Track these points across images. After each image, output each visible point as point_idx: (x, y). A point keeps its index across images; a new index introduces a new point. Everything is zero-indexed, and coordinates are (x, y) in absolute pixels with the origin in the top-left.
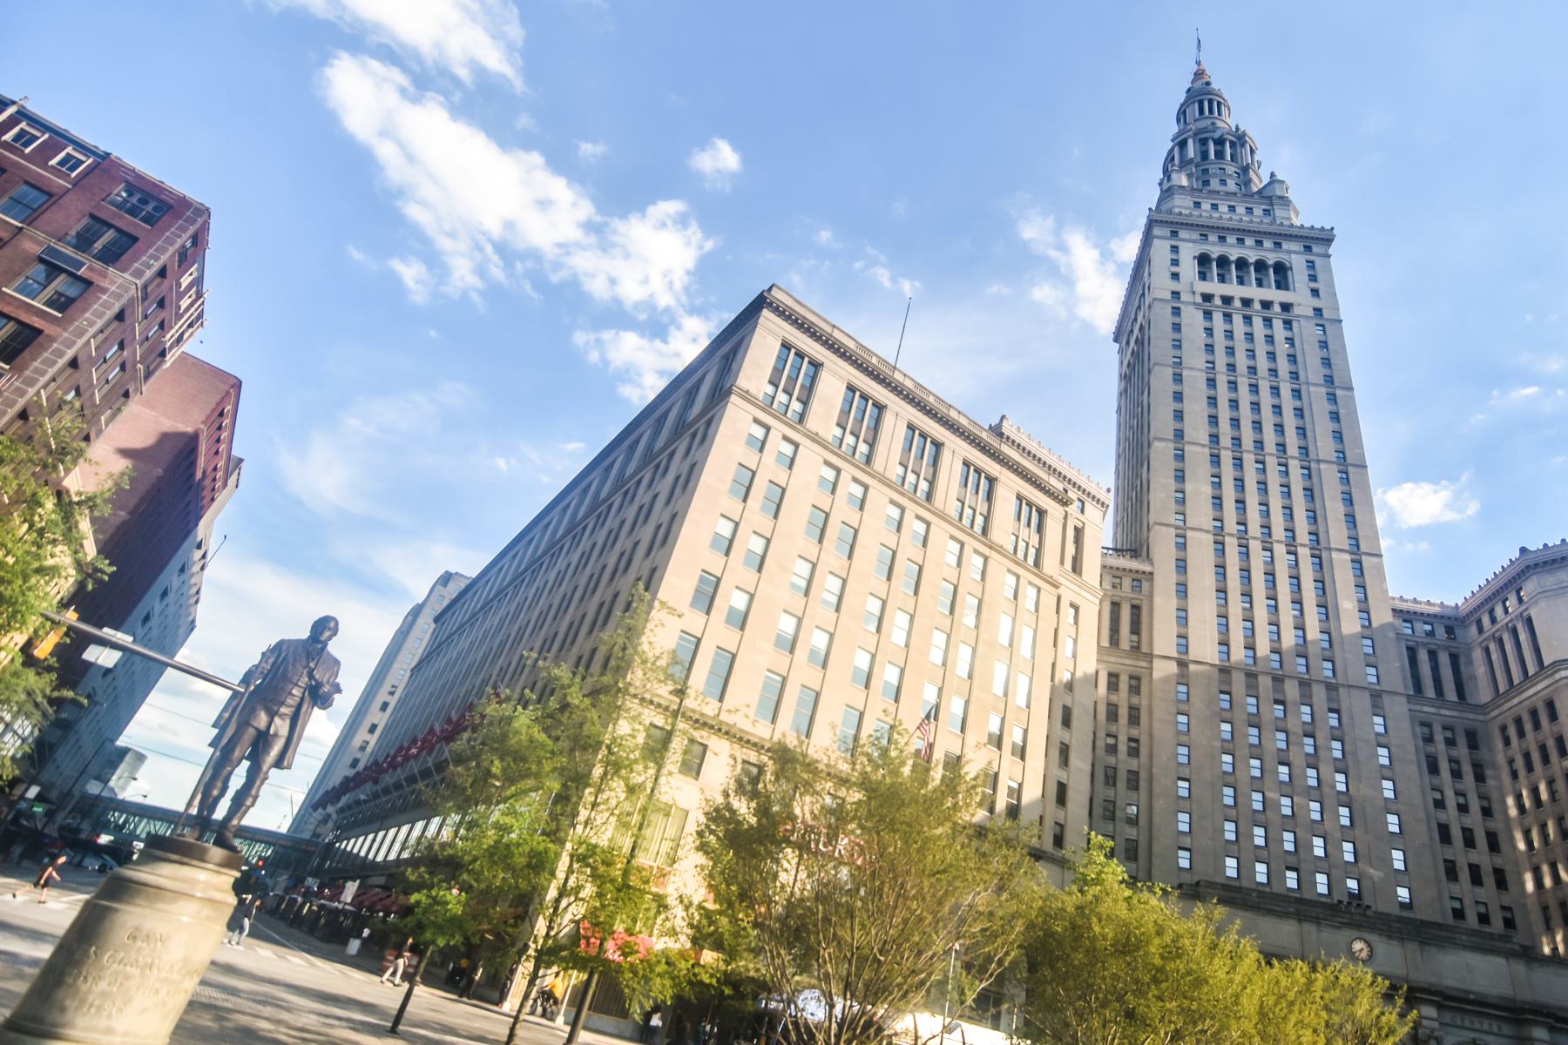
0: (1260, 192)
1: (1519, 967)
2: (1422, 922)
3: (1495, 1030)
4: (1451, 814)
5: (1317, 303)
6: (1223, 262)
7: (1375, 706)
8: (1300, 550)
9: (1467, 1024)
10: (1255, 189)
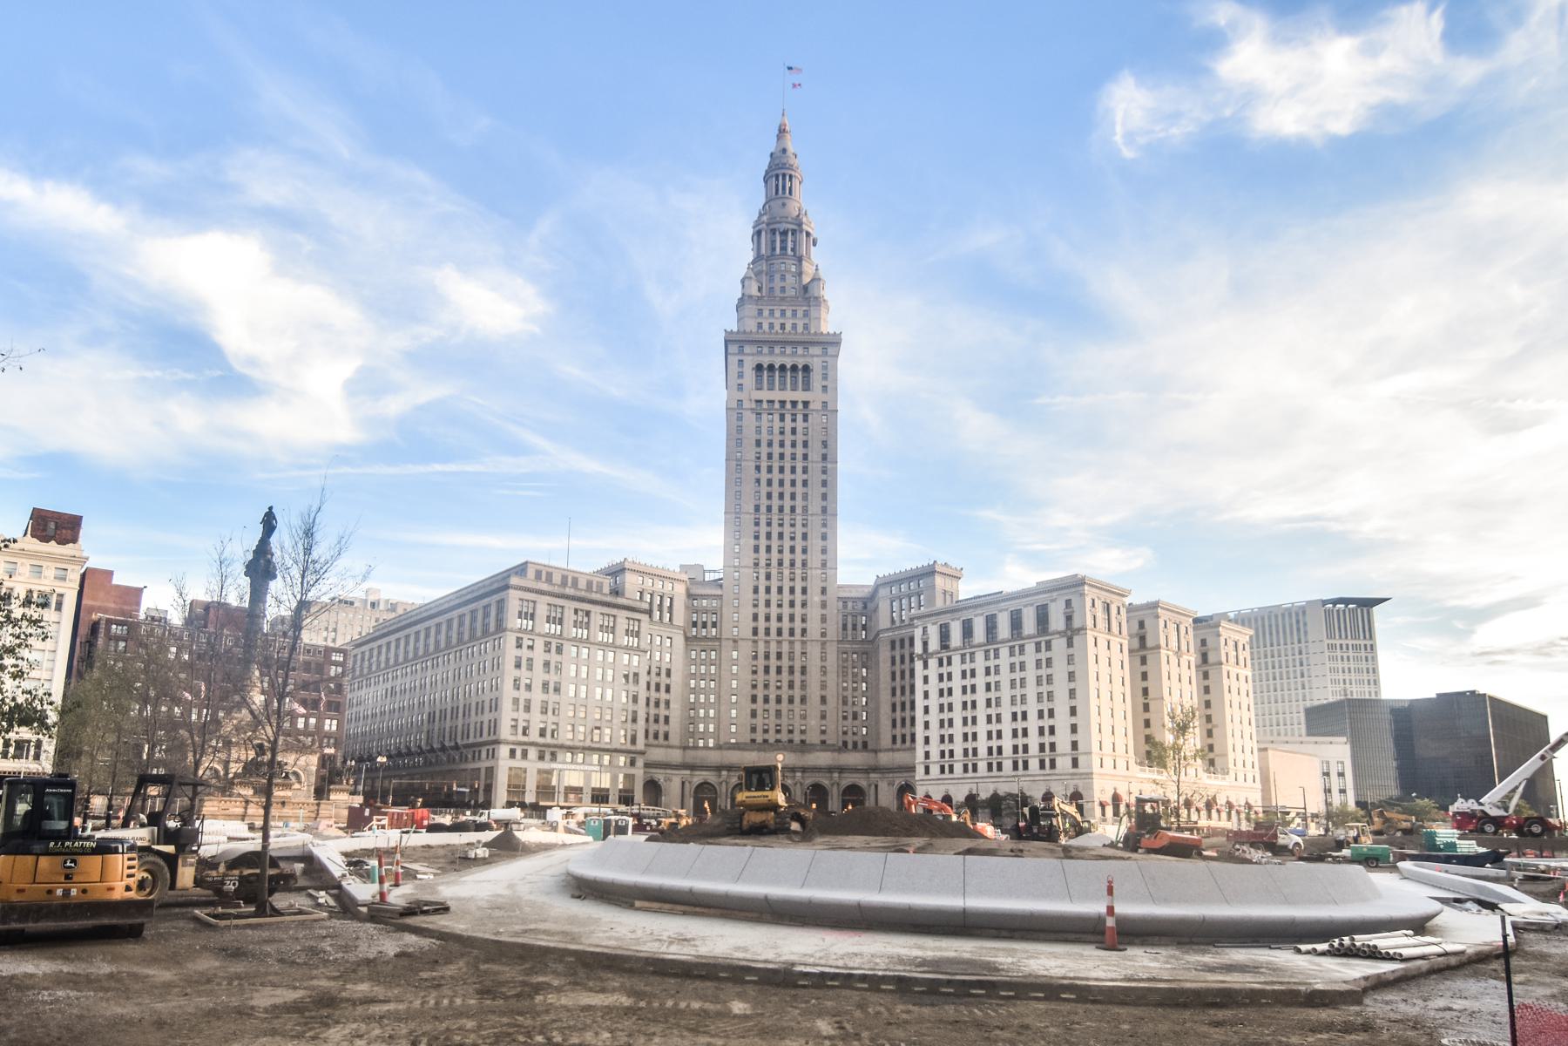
4: (849, 693)
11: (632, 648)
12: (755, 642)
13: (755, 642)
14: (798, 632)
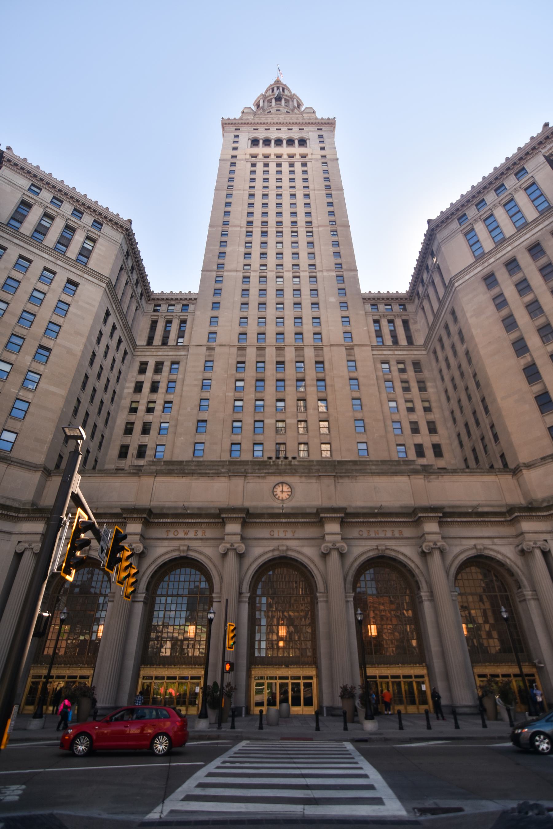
1: (419, 481)
2: (339, 462)
3: (397, 535)
5: (323, 153)
7: (348, 355)
8: (302, 274)
9: (373, 535)
13: (242, 349)
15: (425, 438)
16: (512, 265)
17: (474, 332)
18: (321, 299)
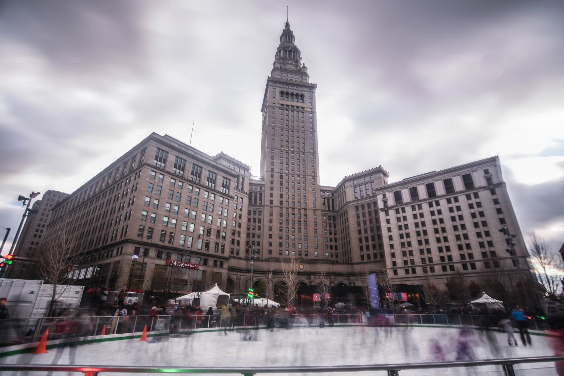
0: (299, 70)
1: (331, 266)
6: (287, 94)
10: (299, 68)
11: (225, 194)
12: (281, 208)
14: (303, 206)
15: (333, 243)
16: (363, 206)
17: (351, 222)
18: (307, 188)
